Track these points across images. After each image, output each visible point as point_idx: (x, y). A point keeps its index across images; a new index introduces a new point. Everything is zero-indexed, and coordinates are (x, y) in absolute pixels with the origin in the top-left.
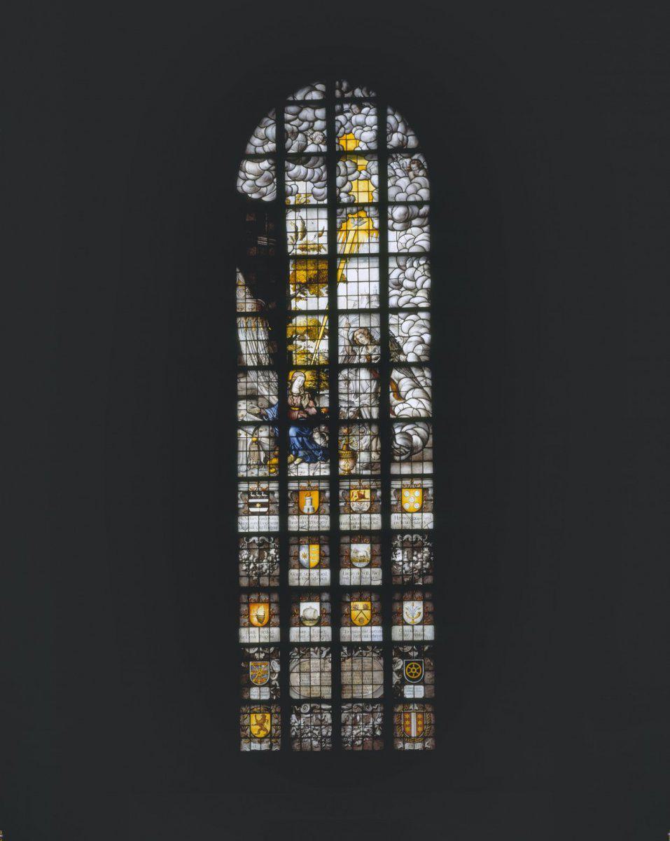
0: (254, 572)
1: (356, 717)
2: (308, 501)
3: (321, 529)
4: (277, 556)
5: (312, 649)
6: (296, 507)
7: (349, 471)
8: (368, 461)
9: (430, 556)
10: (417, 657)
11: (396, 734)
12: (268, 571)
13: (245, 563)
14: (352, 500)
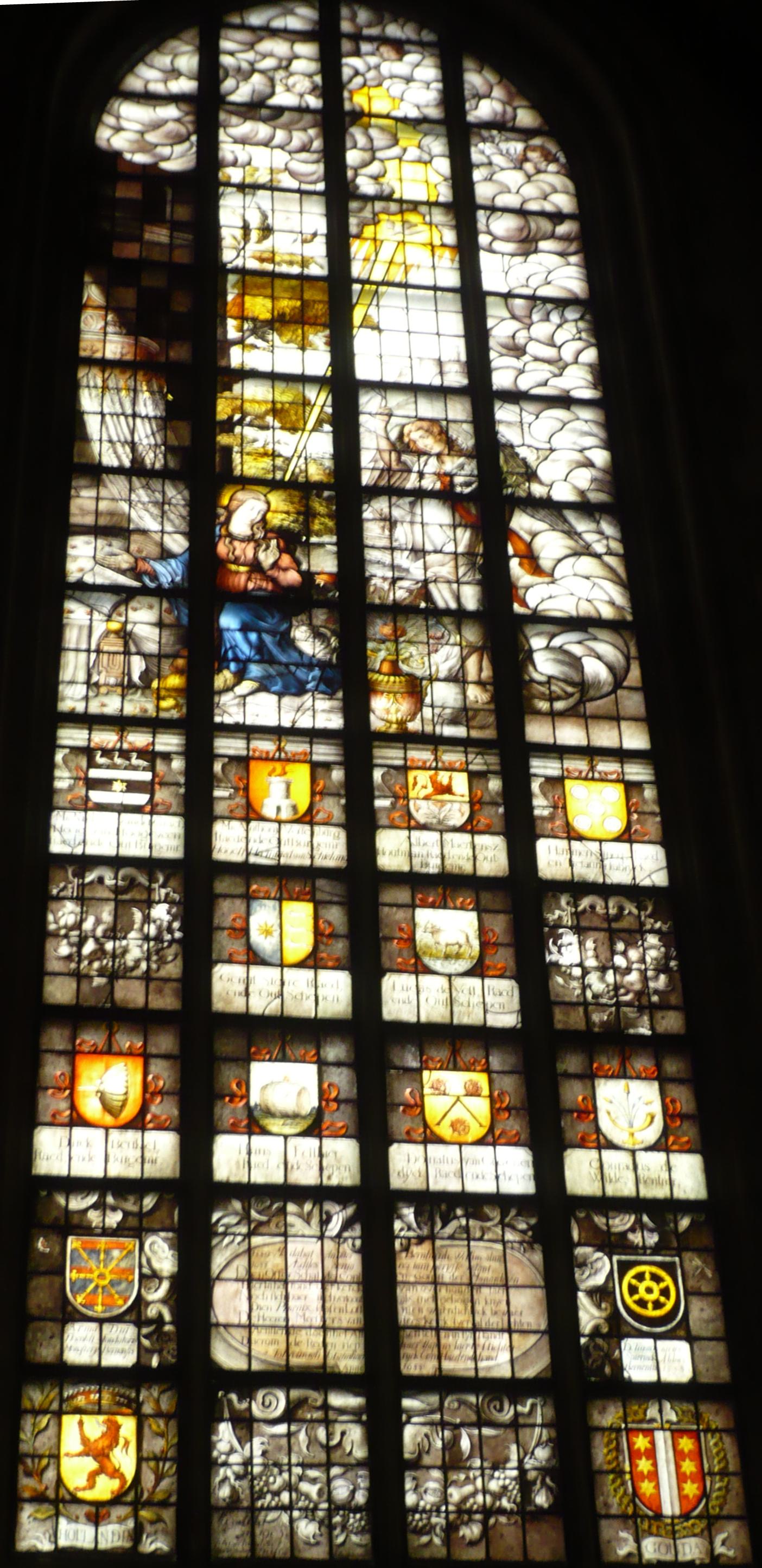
0: (96, 965)
1: (456, 1439)
2: (276, 785)
3: (319, 862)
4: (176, 925)
5: (291, 1207)
6: (240, 800)
7: (402, 723)
8: (459, 704)
9: (667, 957)
10: (656, 1250)
11: (606, 1505)
12: (144, 966)
13: (66, 936)
14: (412, 794)
